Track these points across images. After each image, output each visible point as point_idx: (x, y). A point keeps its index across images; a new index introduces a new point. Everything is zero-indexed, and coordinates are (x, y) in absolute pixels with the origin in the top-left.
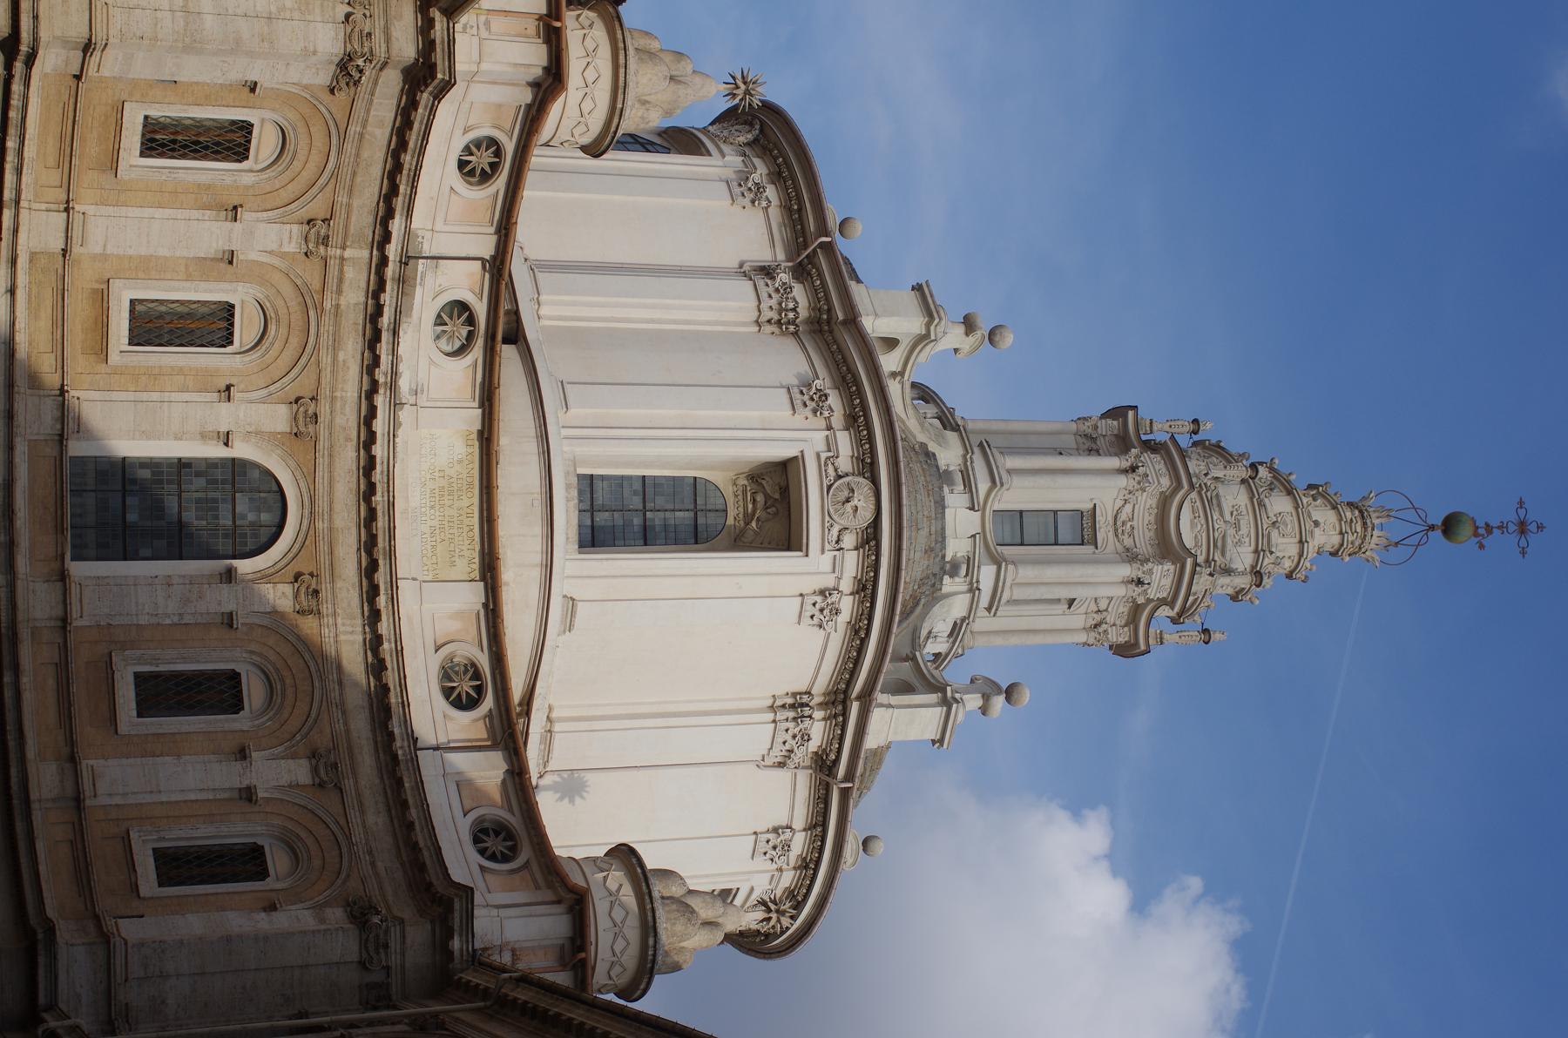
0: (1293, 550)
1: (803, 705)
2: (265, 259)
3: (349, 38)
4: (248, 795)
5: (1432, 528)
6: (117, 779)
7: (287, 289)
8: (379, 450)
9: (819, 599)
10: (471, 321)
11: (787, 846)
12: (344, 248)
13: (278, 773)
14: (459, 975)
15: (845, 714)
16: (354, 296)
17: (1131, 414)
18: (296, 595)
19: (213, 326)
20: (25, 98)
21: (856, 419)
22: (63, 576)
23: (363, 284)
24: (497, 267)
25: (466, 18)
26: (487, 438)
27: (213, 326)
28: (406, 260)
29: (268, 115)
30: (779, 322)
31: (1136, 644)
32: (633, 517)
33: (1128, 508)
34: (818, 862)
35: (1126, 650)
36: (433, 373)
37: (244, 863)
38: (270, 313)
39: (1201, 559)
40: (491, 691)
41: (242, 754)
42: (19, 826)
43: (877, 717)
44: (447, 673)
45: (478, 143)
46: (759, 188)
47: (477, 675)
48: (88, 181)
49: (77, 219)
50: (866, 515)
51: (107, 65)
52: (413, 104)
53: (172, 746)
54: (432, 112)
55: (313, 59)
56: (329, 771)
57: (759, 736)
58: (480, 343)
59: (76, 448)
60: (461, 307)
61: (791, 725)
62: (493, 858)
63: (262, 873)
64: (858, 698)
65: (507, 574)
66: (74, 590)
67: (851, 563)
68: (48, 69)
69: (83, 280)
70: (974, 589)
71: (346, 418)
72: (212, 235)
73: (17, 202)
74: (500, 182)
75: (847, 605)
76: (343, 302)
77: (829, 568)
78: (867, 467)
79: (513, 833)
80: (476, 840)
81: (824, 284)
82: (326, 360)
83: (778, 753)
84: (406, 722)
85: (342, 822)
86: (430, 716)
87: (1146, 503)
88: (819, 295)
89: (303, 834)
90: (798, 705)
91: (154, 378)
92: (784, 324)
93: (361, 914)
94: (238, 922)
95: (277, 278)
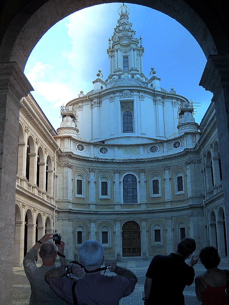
0: (128, 26)
1: (155, 100)
2: (95, 178)
3: (66, 167)
4: (170, 179)
5: (124, 4)
6: (168, 197)
7: (99, 174)
8: (121, 161)
9: (140, 98)
10: (102, 148)
11: (174, 102)
12: (93, 167)
13: (167, 175)
14: (196, 151)
15: (157, 94)
16: (99, 165)
17: (108, 50)
18: (142, 172)
19: (104, 185)
20: (76, 210)
21: (114, 92)
22: (140, 204)
23: (98, 164)
24: (95, 145)
25: (62, 150)
26: (119, 146)
27: (104, 185)
28: (95, 158)
29: (76, 177)
30: (100, 104)
31: (142, 49)
32: (128, 124)
33: (123, 51)
34: (177, 98)
35: (143, 51)
36: (110, 155)
37: (180, 179)
38: (103, 177)
39: (130, 40)
40: (155, 144)
41: (164, 180)
42: (175, 209)
43: (156, 90)
44: (153, 152)
45: (78, 148)
46: (80, 106)
47: (153, 147)
48: (85, 202)
49: (91, 203)
50: (129, 91)
51: (70, 199)
52: (74, 157)
53: (163, 189)
54: (75, 155)
55: (69, 172)
56: (168, 168)
57: (160, 107)
58: (106, 147)
59: (122, 203)
60: (100, 150)
61: (158, 102)
62: (179, 145)
63: (181, 177)
64: (154, 92)
65: (138, 143)
66: (142, 202)
67: (135, 93)
68: (72, 207)
69: (99, 202)
70: (136, 74)
71: (116, 166)
72: (92, 185)
73: (90, 211)
74: (83, 145)
75: (141, 94)
76: (101, 166)
77: (136, 97)
78: (121, 91)
79: (176, 142)
80: (176, 147)
81: (94, 97)
82: (109, 169)
83: (162, 104)
84: (159, 157)
85: (174, 166)
86: (159, 154)
87: (122, 48)
88: (95, 98)
89: (176, 171)
90: (155, 101)
91: (112, 193)
92: (100, 103)
93: (188, 163)
94: (189, 180)
95: (98, 176)
